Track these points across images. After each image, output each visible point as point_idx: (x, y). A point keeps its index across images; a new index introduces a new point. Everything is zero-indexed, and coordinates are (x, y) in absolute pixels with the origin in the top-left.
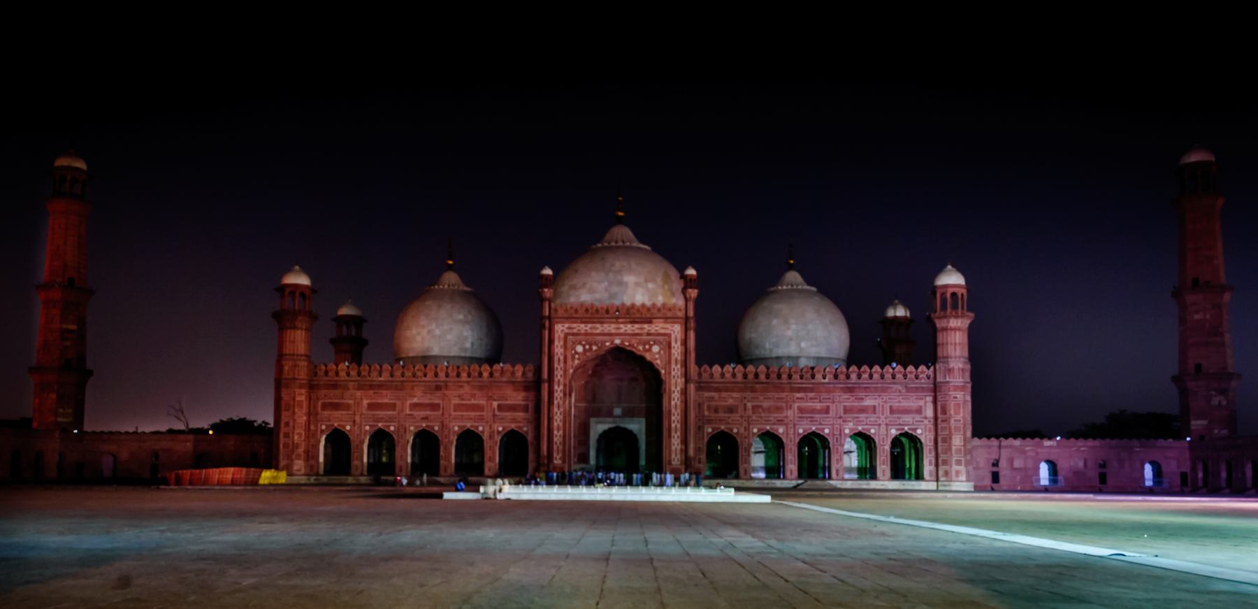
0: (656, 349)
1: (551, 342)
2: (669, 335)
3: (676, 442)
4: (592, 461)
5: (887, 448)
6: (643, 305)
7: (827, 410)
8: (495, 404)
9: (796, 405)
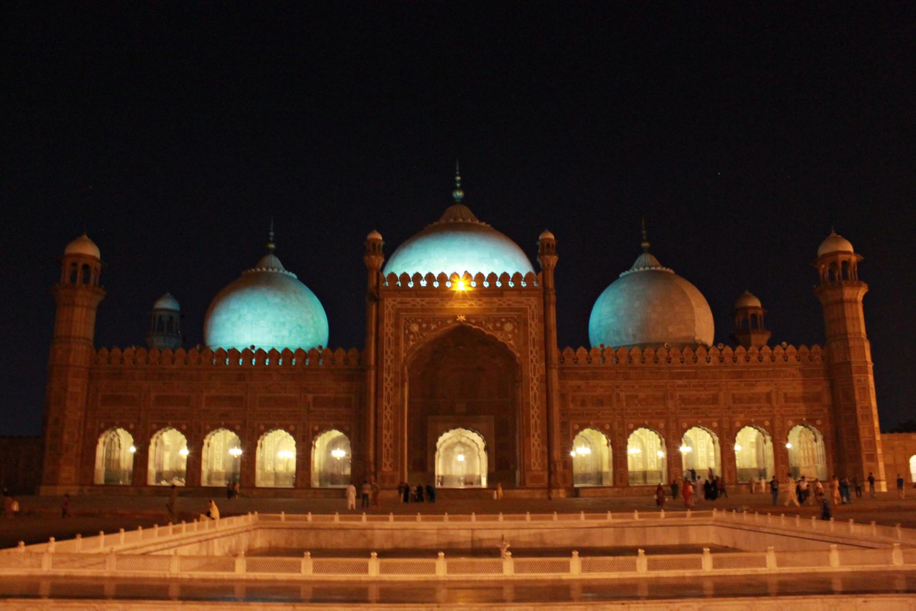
0: (508, 327)
1: (379, 320)
2: (525, 311)
7: (715, 399)
8: (310, 397)
9: (678, 394)
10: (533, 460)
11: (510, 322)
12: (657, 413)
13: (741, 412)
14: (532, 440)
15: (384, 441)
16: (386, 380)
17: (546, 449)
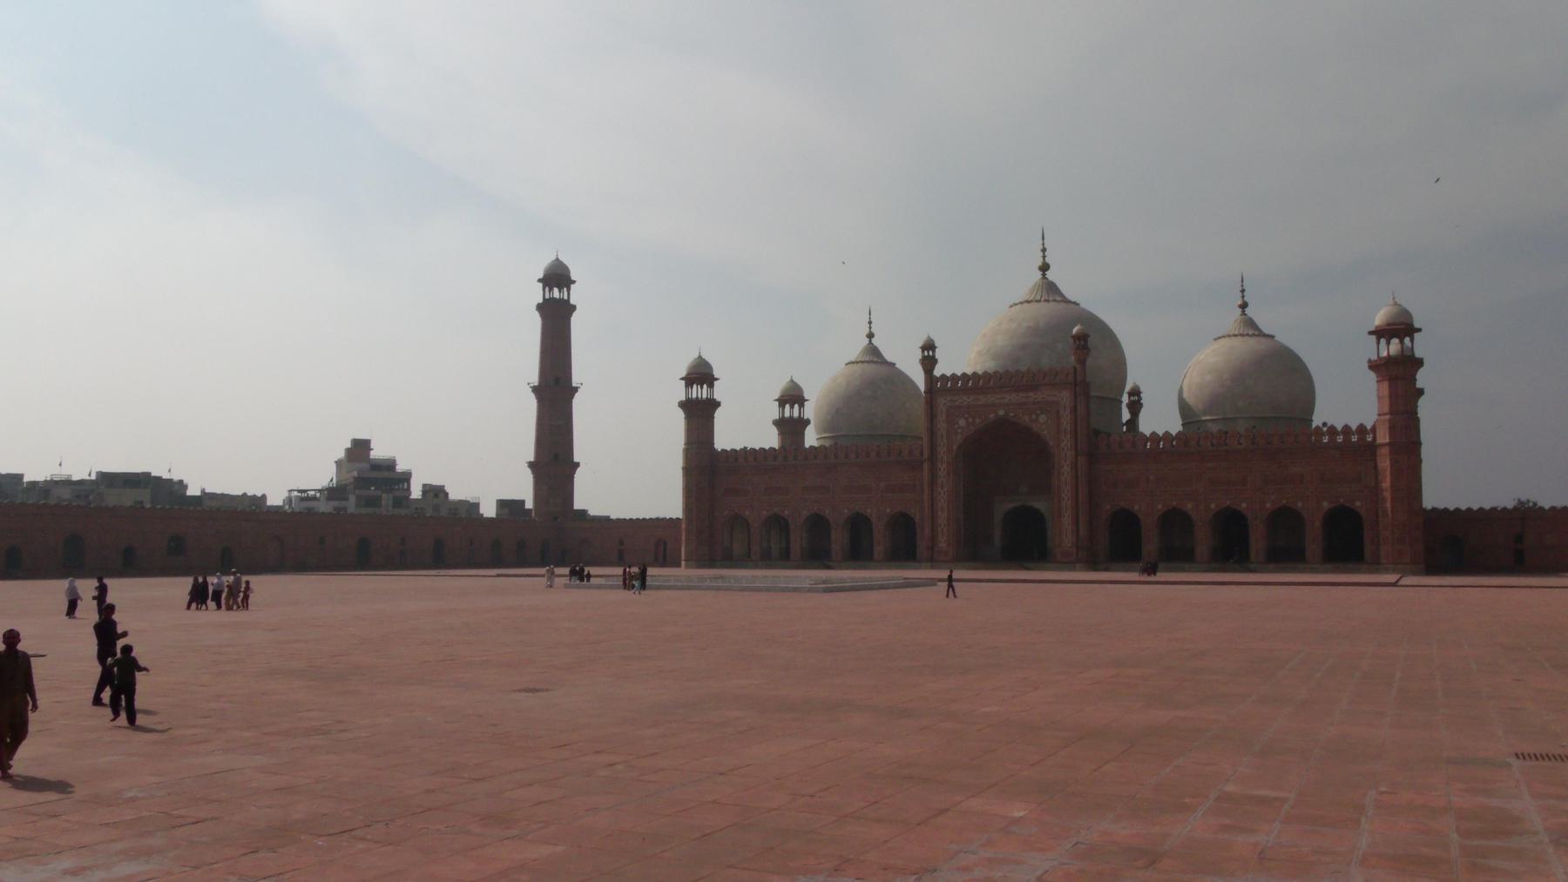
0: (1042, 418)
3: (1067, 521)
4: (997, 540)
5: (1318, 523)
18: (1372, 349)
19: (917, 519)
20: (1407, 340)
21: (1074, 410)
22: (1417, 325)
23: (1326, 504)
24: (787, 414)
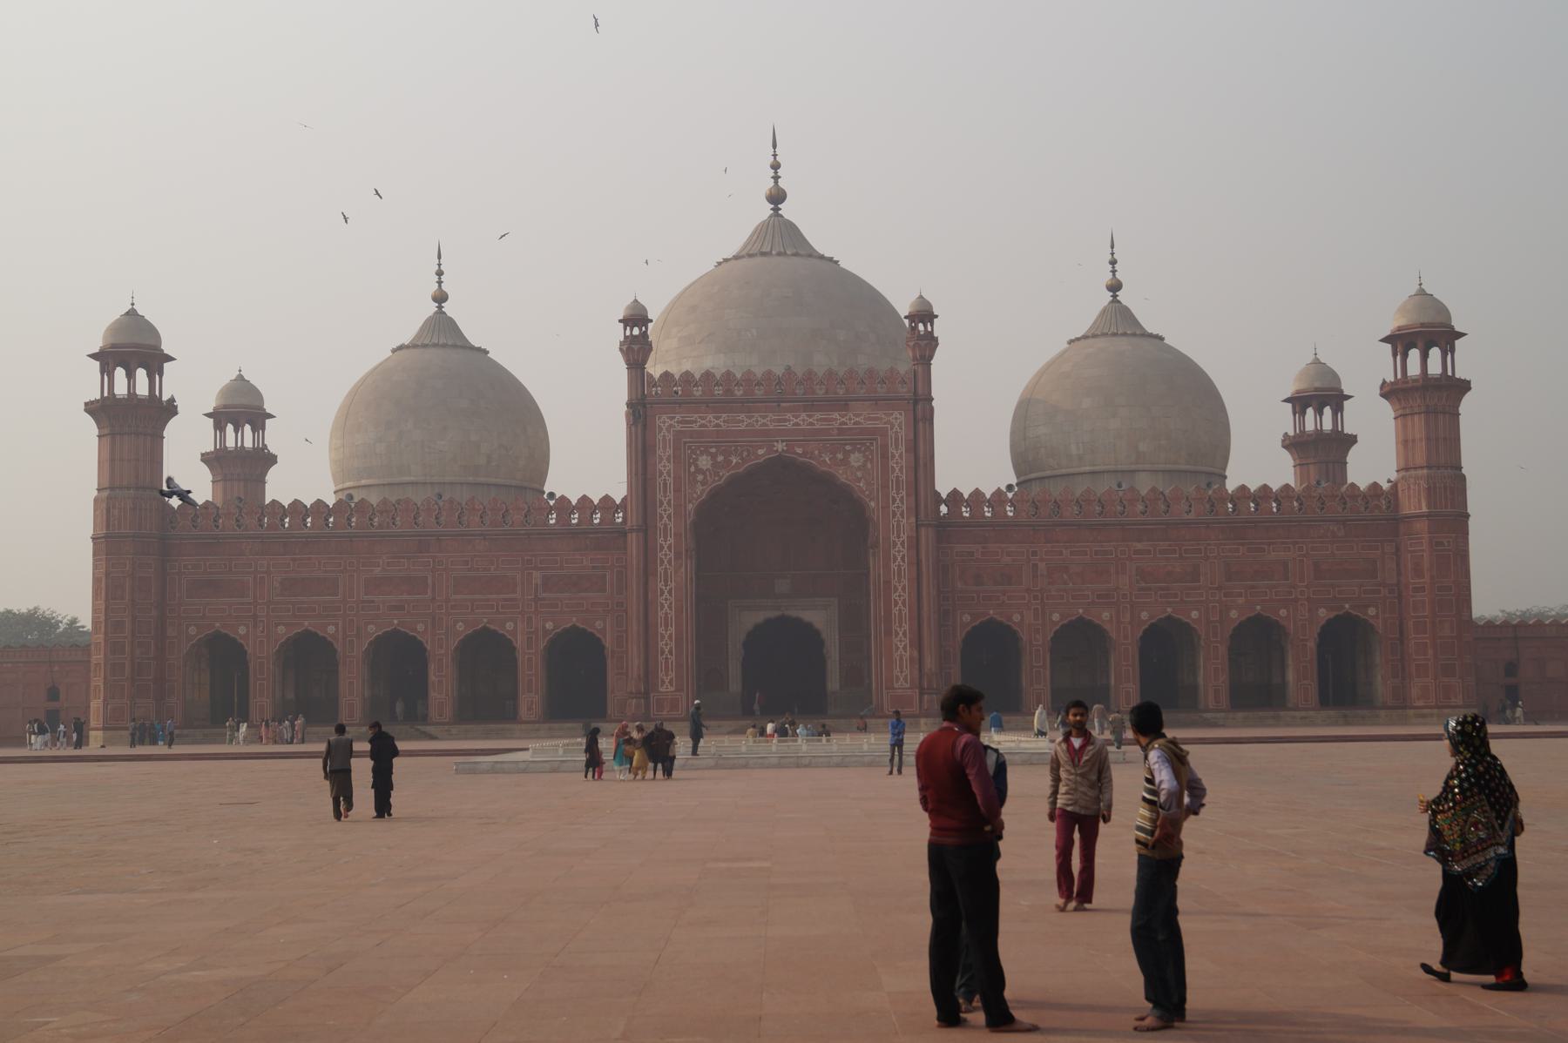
0: (856, 459)
4: (735, 686)
5: (1312, 644)
6: (830, 374)
8: (537, 576)
10: (896, 672)
11: (859, 450)
12: (1099, 596)
13: (1240, 595)
14: (895, 640)
15: (661, 644)
16: (662, 548)
17: (916, 654)
18: (1383, 365)
19: (608, 643)
20: (1435, 353)
21: (913, 447)
22: (1457, 329)
23: (1323, 614)
24: (230, 443)
